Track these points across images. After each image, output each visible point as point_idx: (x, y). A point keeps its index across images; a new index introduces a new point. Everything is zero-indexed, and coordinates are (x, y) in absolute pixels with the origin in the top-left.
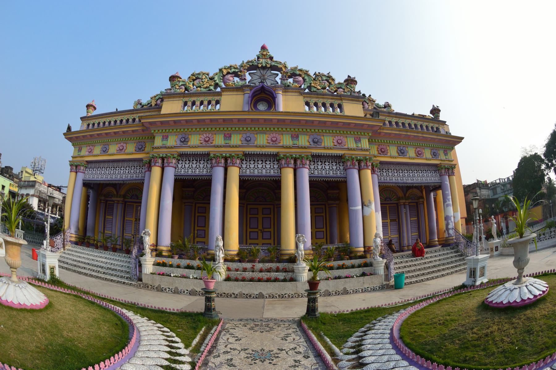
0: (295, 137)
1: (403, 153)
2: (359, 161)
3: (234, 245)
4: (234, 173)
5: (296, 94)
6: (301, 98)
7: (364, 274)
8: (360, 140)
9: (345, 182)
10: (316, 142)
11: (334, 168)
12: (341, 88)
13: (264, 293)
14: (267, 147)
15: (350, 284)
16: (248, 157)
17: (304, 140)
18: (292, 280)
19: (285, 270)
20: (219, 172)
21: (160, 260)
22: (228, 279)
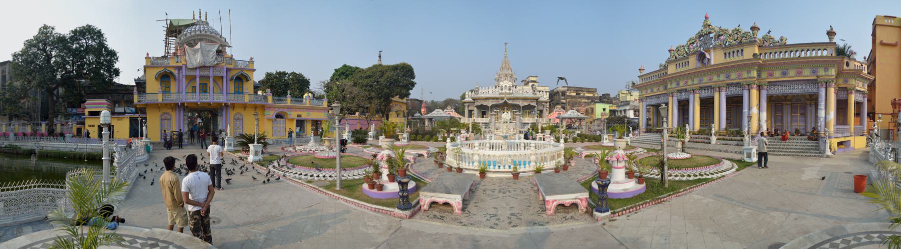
0: (718, 76)
1: (784, 74)
2: (748, 85)
3: (697, 127)
4: (697, 96)
5: (719, 49)
6: (722, 51)
7: (738, 145)
8: (750, 72)
9: (742, 97)
10: (728, 77)
11: (738, 89)
12: (744, 37)
13: (699, 148)
14: (708, 83)
15: (729, 148)
16: (701, 88)
17: (722, 77)
18: (710, 143)
19: (707, 139)
20: (691, 97)
21: (671, 135)
22: (689, 141)
